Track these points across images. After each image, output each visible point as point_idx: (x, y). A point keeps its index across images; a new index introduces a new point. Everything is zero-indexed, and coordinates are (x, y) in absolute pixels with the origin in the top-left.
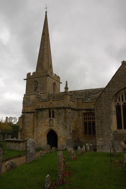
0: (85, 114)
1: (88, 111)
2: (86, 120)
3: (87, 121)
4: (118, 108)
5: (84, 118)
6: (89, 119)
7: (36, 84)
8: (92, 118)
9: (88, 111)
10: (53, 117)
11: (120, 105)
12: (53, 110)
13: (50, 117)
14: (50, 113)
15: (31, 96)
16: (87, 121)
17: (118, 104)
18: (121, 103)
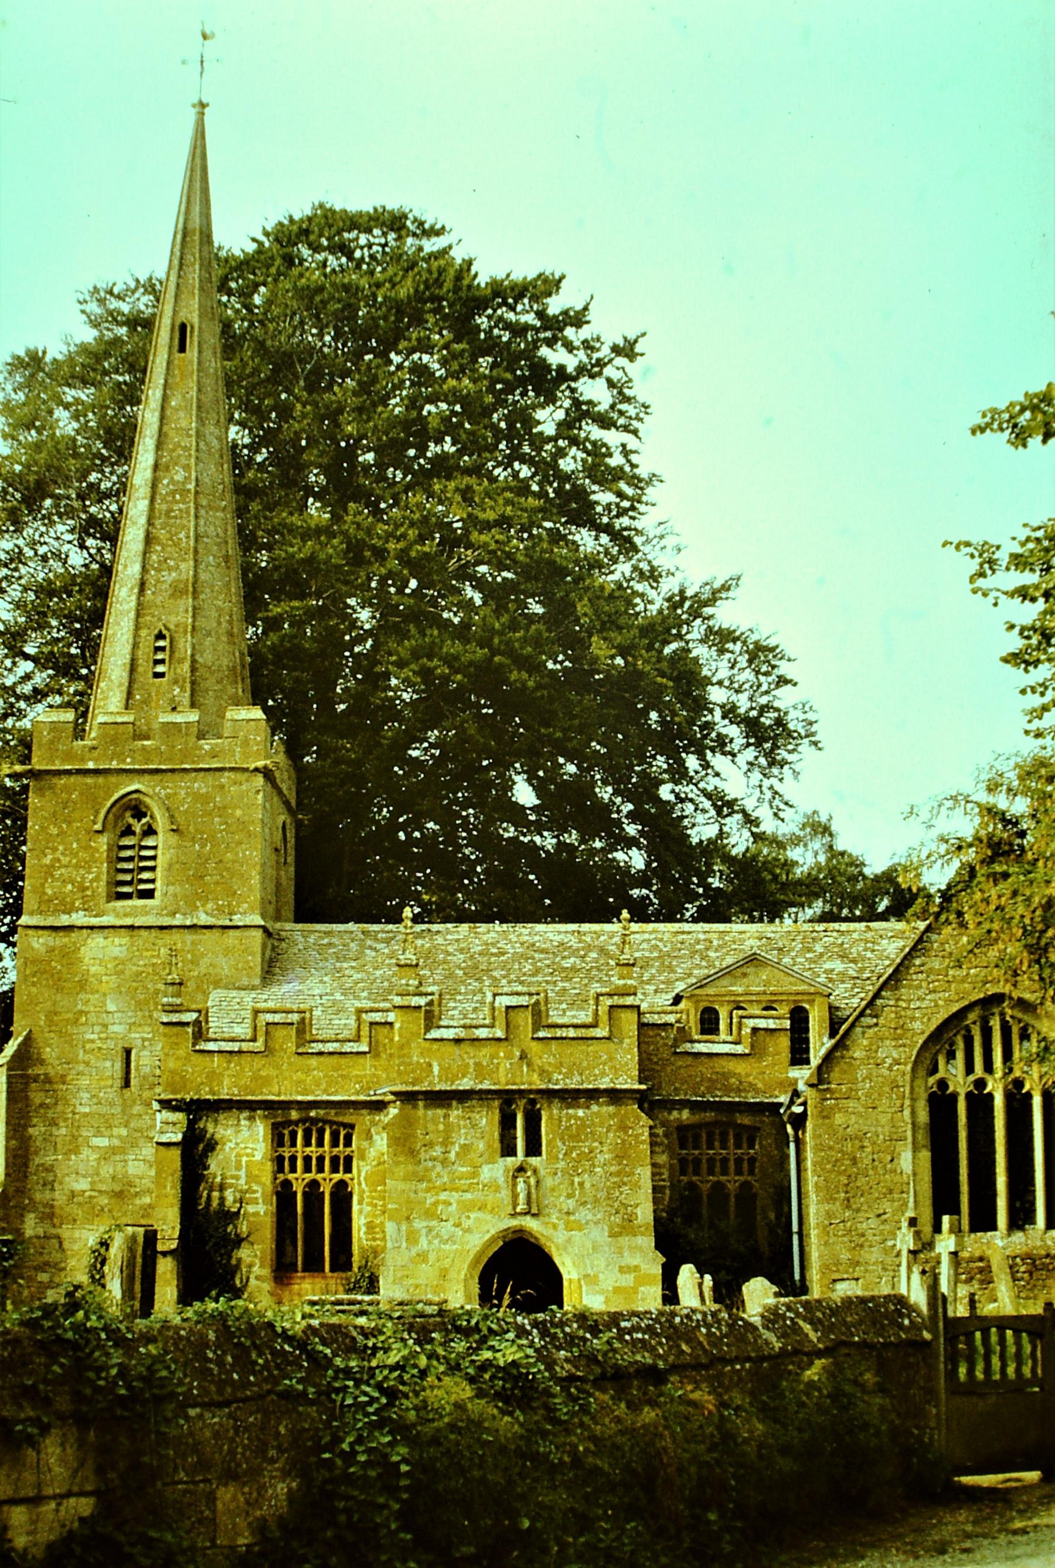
0: (684, 1135)
1: (709, 1116)
2: (697, 1173)
3: (705, 1183)
4: (941, 1103)
5: (683, 1162)
6: (745, 1165)
7: (128, 831)
8: (711, 1161)
9: (709, 1116)
10: (533, 1148)
11: (954, 1096)
12: (533, 1102)
13: (508, 1150)
14: (507, 1123)
15: (97, 940)
16: (705, 1183)
17: (943, 1084)
18: (960, 1083)
